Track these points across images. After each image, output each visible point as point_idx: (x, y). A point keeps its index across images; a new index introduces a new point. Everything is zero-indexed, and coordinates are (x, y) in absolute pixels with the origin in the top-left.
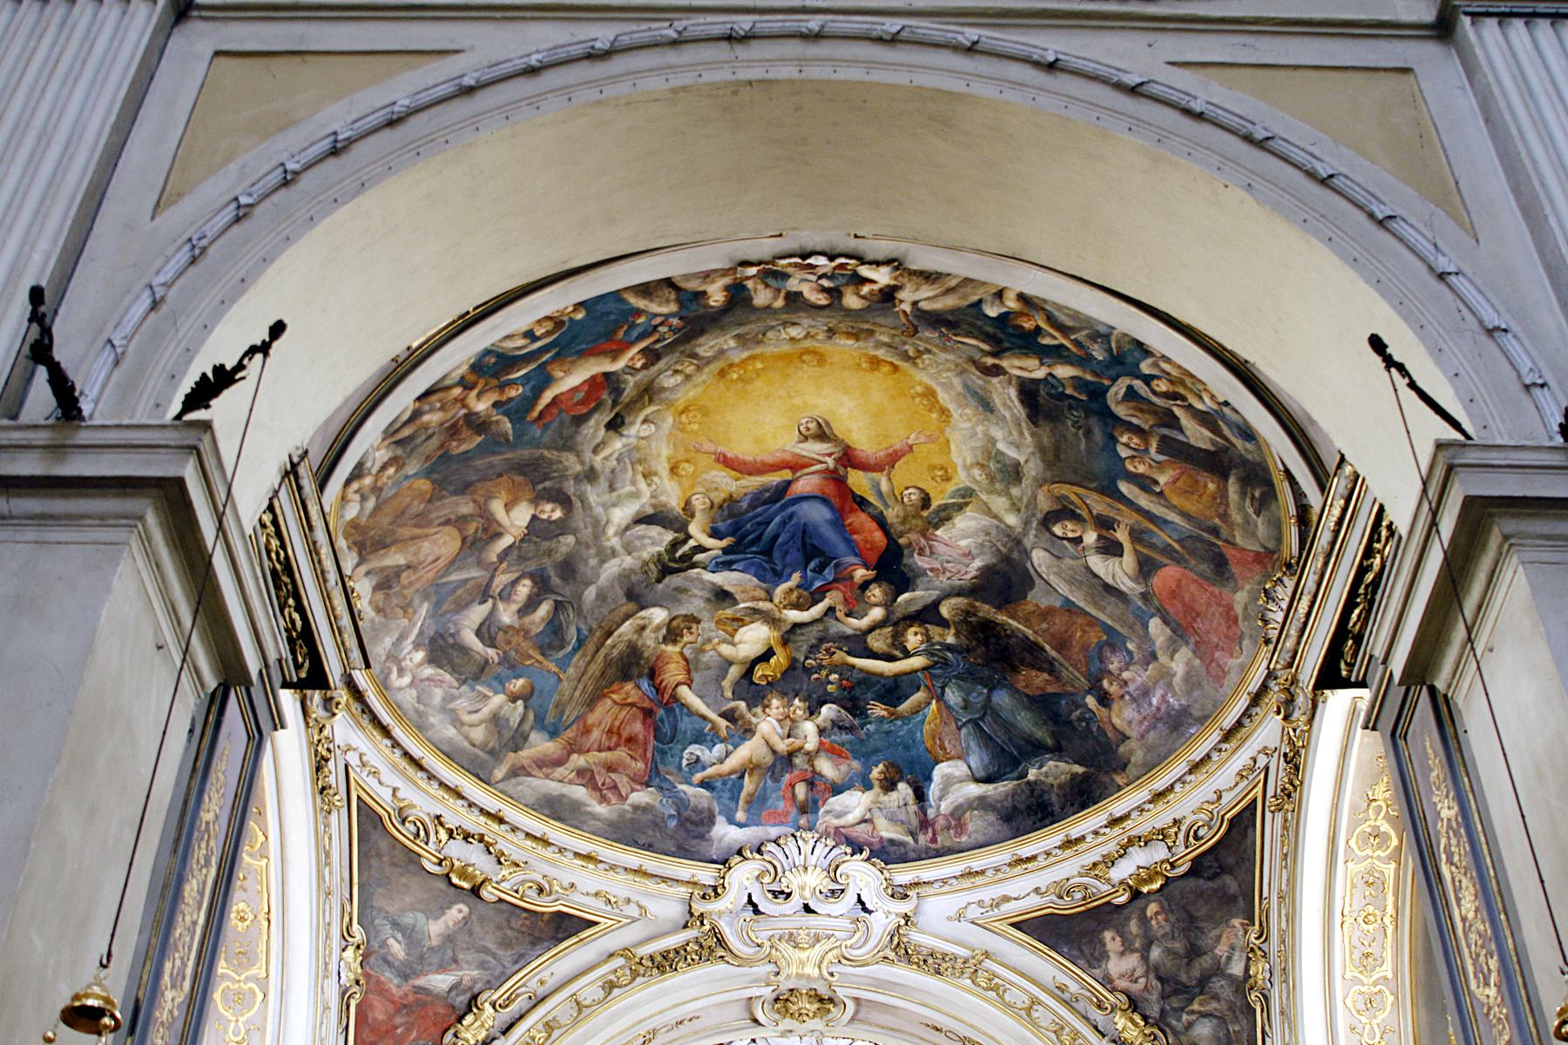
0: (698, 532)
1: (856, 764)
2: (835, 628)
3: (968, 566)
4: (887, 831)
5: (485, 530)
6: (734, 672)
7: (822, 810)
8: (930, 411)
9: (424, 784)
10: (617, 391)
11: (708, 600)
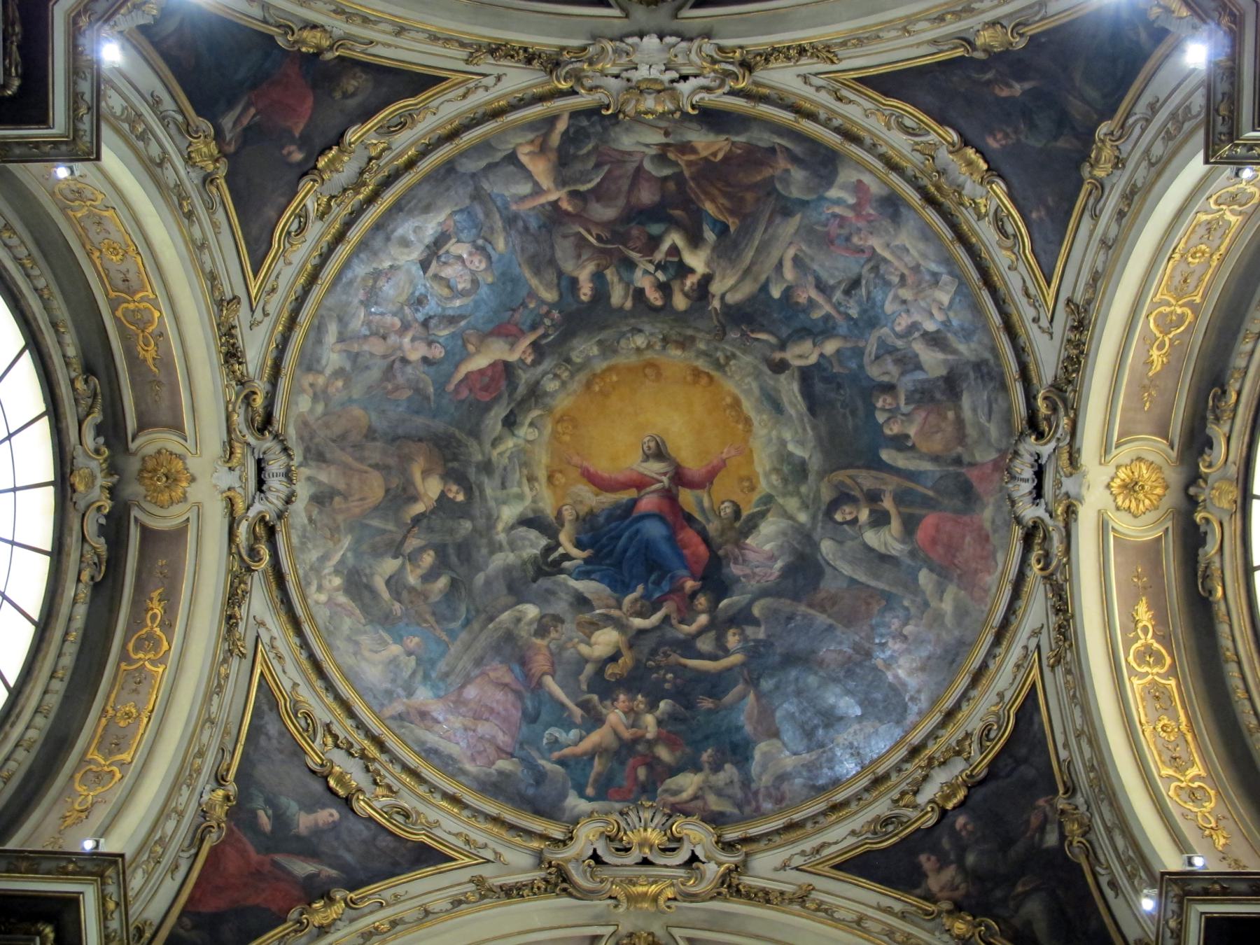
0: (567, 546)
1: (688, 750)
2: (670, 633)
3: (771, 568)
4: (714, 803)
5: (404, 489)
6: (589, 669)
7: (660, 790)
8: (737, 422)
9: (323, 693)
10: (513, 386)
11: (571, 605)
